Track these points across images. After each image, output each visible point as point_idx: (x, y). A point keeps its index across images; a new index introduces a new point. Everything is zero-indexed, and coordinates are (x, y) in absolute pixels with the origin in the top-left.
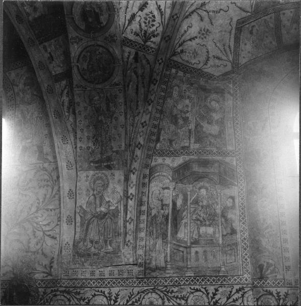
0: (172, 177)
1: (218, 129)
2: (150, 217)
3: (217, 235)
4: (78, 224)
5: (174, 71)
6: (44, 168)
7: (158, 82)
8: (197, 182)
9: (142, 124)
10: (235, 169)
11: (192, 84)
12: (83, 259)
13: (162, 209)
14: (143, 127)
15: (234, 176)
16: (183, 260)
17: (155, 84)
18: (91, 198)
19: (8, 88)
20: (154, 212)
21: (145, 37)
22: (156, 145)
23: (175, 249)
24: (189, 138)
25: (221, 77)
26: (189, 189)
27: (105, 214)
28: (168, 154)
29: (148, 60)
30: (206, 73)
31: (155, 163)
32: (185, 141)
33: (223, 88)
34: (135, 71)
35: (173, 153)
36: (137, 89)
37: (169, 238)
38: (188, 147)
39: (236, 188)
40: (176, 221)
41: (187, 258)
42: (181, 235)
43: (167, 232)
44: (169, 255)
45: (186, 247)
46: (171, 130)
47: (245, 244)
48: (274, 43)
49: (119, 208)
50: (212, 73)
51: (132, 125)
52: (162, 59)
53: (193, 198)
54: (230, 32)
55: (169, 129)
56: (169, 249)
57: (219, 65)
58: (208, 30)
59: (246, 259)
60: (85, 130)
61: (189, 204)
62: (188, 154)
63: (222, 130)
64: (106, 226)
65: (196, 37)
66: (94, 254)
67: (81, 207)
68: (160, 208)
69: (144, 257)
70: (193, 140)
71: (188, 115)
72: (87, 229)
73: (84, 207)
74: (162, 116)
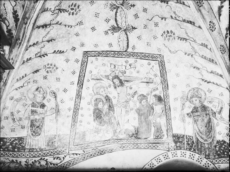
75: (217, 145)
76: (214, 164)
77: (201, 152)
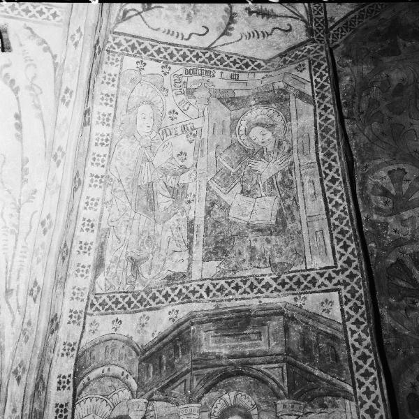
0: (138, 380)
1: (276, 207)
5: (130, 62)
7: (74, 94)
8: (214, 394)
10: (341, 336)
11: (190, 93)
15: (336, 358)
17: (67, 104)
22: (94, 282)
24: (190, 248)
25: (278, 59)
28: (129, 303)
29: (44, 42)
31: (94, 337)
32: (176, 256)
33: (282, 85)
34: (7, 75)
36: (19, 127)
39: (351, 406)
46: (135, 229)
50: (249, 54)
51: (12, 232)
55: (129, 227)
57: (269, 32)
63: (289, 208)
70: (198, 252)
71: (184, 179)
74: (108, 190)
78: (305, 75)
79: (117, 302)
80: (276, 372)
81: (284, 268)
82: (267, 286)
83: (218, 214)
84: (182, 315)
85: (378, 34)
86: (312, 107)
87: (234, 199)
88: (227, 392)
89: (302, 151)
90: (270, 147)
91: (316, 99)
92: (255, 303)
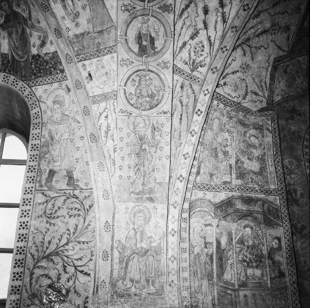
2: (192, 255)
3: (265, 278)
4: (116, 261)
6: (74, 195)
7: (203, 114)
9: (184, 155)
10: (279, 209)
11: (231, 118)
12: (122, 300)
13: (206, 247)
14: (185, 159)
16: (232, 304)
18: (130, 232)
19: (33, 104)
20: (197, 250)
21: (193, 66)
22: (196, 179)
23: (222, 292)
24: (231, 173)
26: (234, 228)
27: (147, 251)
28: (209, 188)
29: (194, 90)
30: (244, 107)
33: (262, 124)
35: (213, 188)
36: (181, 119)
37: (215, 279)
38: (229, 183)
39: (281, 228)
40: (221, 260)
41: (236, 302)
42: (227, 276)
43: (213, 273)
44: (216, 298)
45: (234, 290)
47: (294, 288)
48: (305, 84)
49: (162, 244)
52: (207, 90)
53: (238, 238)
54: (267, 69)
56: (216, 291)
57: (256, 100)
58: (248, 65)
59: (297, 305)
60: (126, 157)
61: (234, 243)
62: (231, 191)
63: (264, 167)
64: (148, 265)
65: (238, 71)
66: (135, 295)
67: (119, 241)
68: (203, 246)
69: (189, 299)
70: (234, 176)
71: (227, 149)
72: (126, 268)
73: (123, 242)
74: (202, 147)
75: (33, 61)
76: (30, 87)
77: (17, 73)
78: (269, 122)
79: (204, 187)
80: (260, 216)
81: (262, 187)
82: (257, 191)
83: (239, 164)
84: (230, 195)
85: (288, 110)
86: (271, 135)
87: (245, 159)
88: (246, 221)
89: (269, 149)
90: (257, 145)
91: (273, 132)
92: (253, 195)
